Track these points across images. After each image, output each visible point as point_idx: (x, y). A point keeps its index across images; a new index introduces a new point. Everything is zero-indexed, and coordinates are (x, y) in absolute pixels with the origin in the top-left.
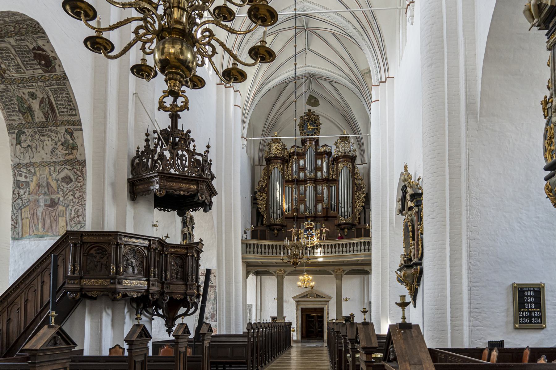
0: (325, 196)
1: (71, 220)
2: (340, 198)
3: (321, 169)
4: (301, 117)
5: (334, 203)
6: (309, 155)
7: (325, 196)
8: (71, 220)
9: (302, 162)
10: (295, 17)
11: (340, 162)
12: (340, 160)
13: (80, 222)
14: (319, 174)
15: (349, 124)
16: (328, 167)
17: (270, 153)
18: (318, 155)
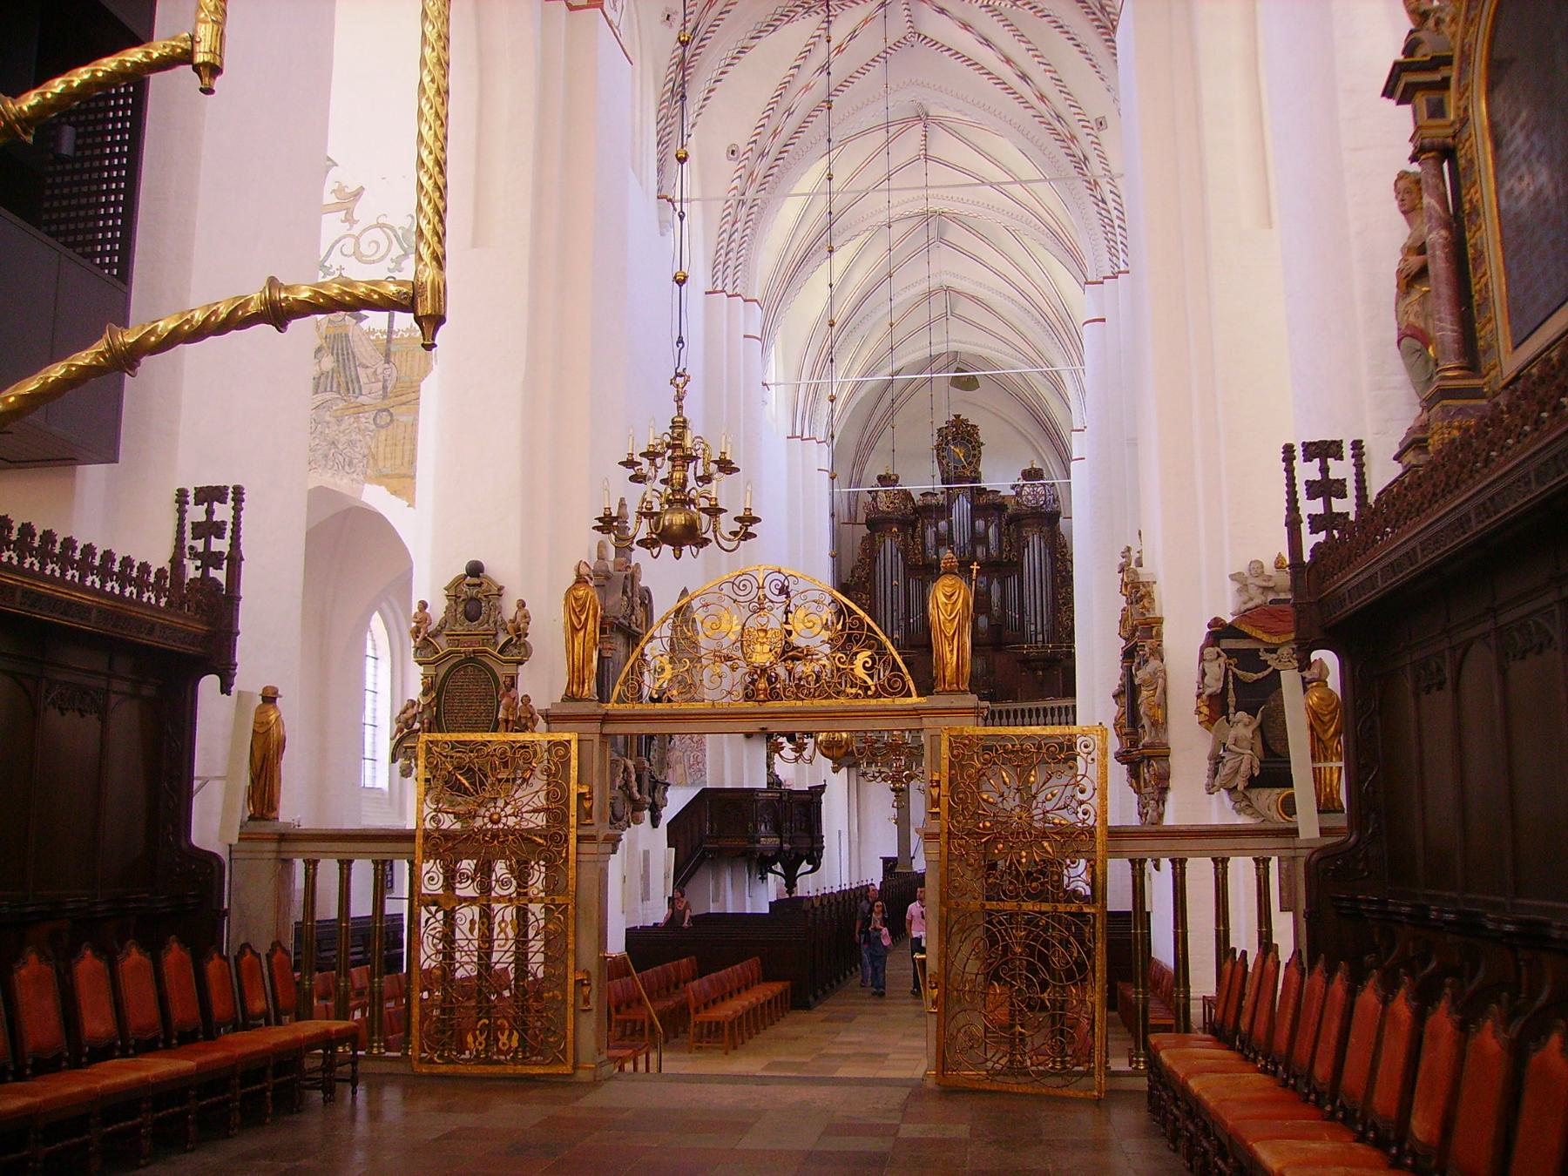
0: (995, 598)
1: (690, 768)
2: (1026, 601)
3: (984, 540)
4: (939, 430)
5: (1013, 614)
6: (961, 508)
7: (995, 598)
8: (690, 768)
9: (943, 524)
10: (930, 294)
11: (1029, 525)
12: (1024, 522)
13: (700, 770)
14: (980, 551)
15: (1046, 430)
16: (1000, 534)
17: (876, 508)
18: (977, 511)
